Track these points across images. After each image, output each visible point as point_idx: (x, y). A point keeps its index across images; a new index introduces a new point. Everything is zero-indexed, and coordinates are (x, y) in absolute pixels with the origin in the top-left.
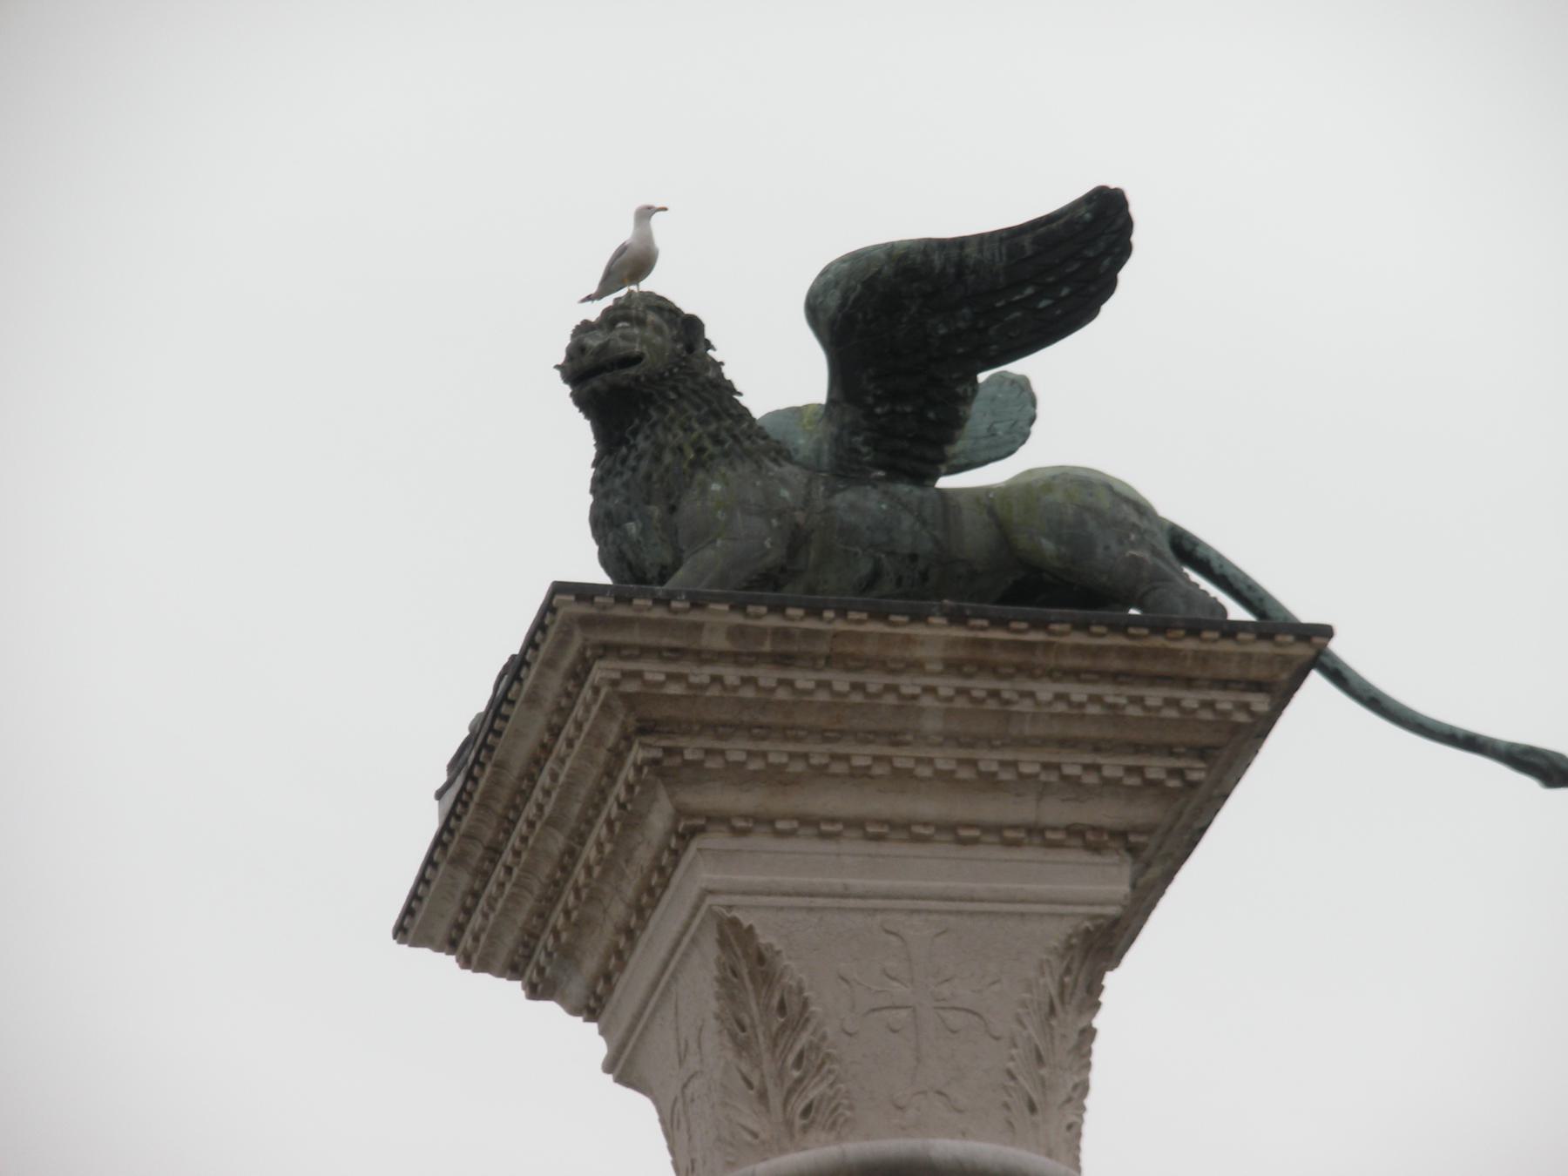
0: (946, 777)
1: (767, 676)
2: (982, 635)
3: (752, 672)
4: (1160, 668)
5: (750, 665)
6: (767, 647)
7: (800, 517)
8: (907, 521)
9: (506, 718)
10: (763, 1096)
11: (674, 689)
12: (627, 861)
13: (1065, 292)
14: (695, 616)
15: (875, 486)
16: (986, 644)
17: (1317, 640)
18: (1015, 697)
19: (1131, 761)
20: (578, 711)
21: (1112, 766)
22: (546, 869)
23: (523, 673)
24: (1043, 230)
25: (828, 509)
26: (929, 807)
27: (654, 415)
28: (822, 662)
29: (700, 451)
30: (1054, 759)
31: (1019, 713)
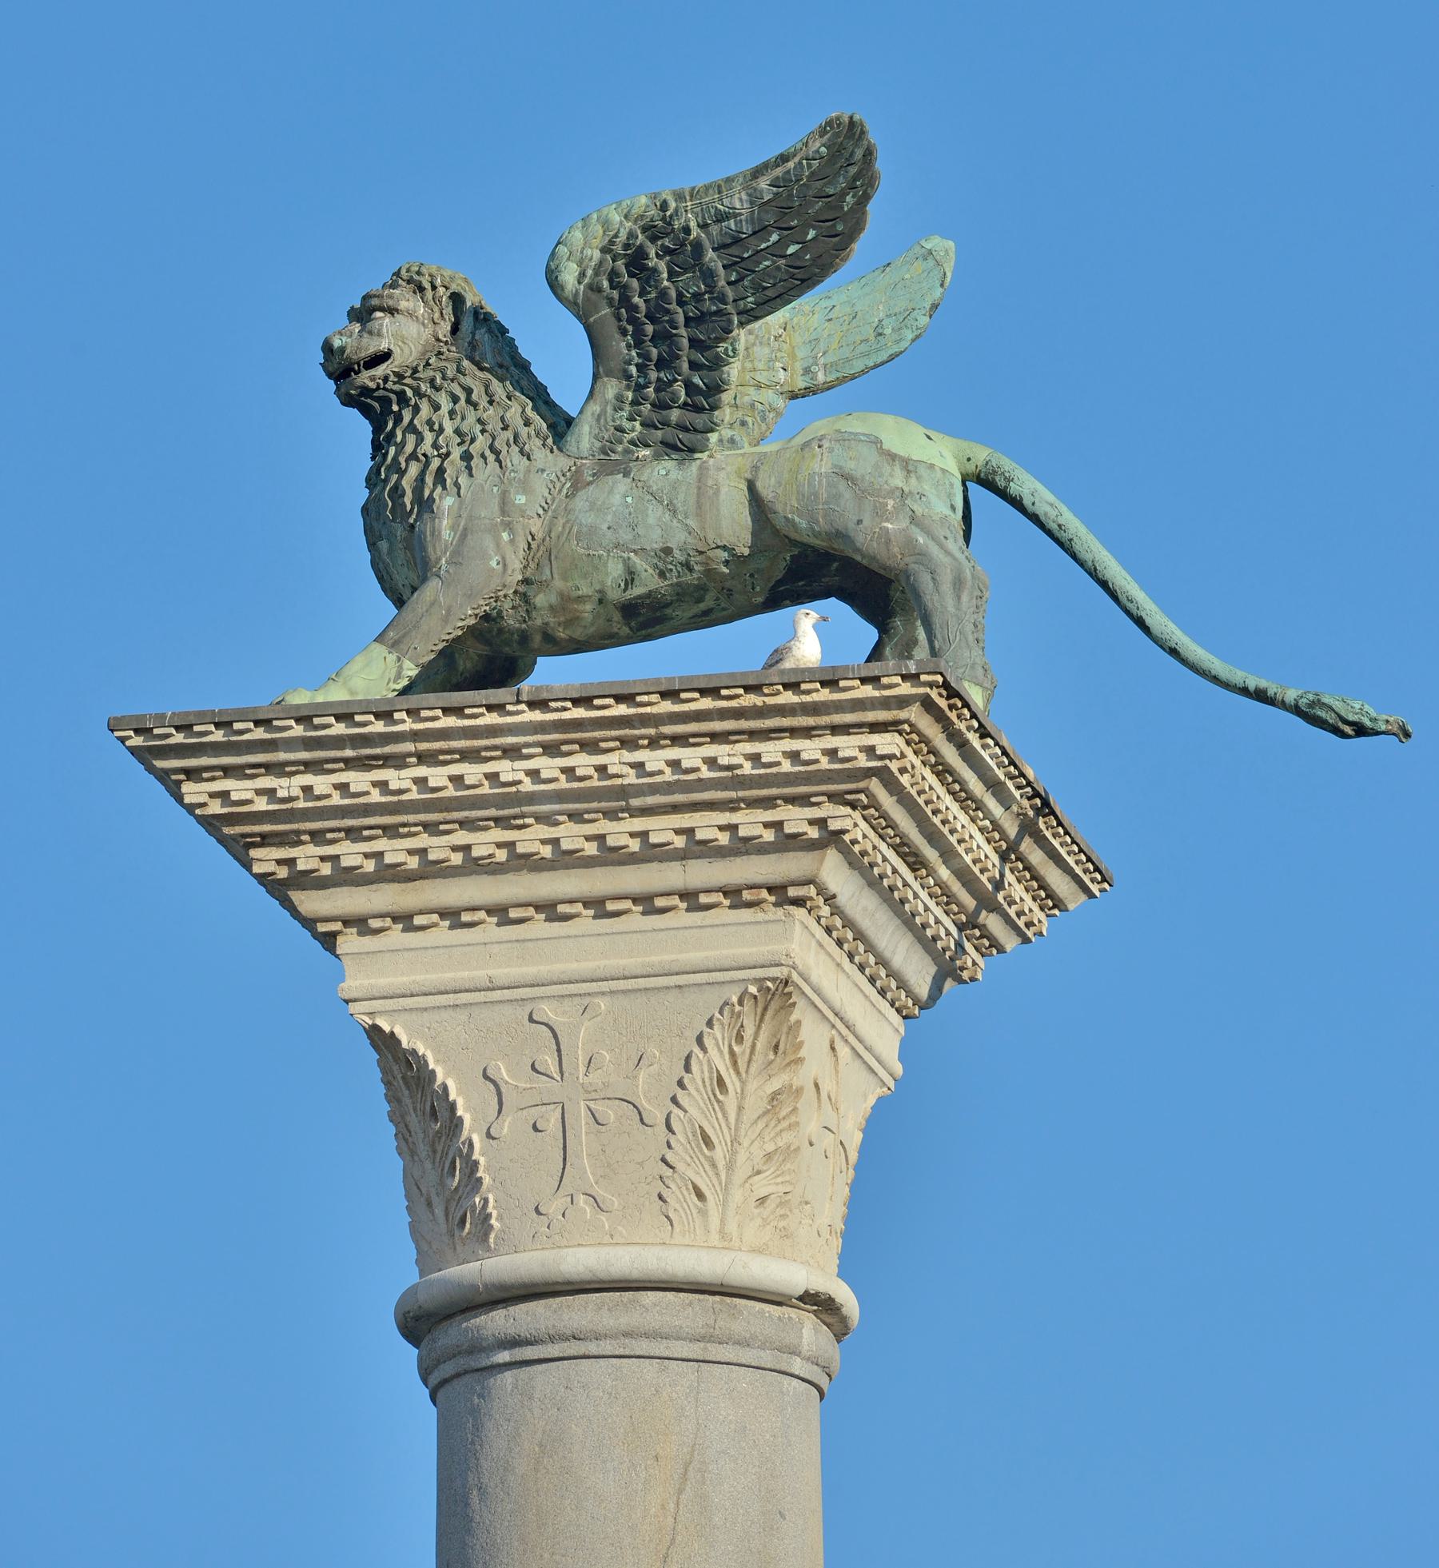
2: (566, 715)
8: (654, 514)
10: (429, 1204)
13: (812, 234)
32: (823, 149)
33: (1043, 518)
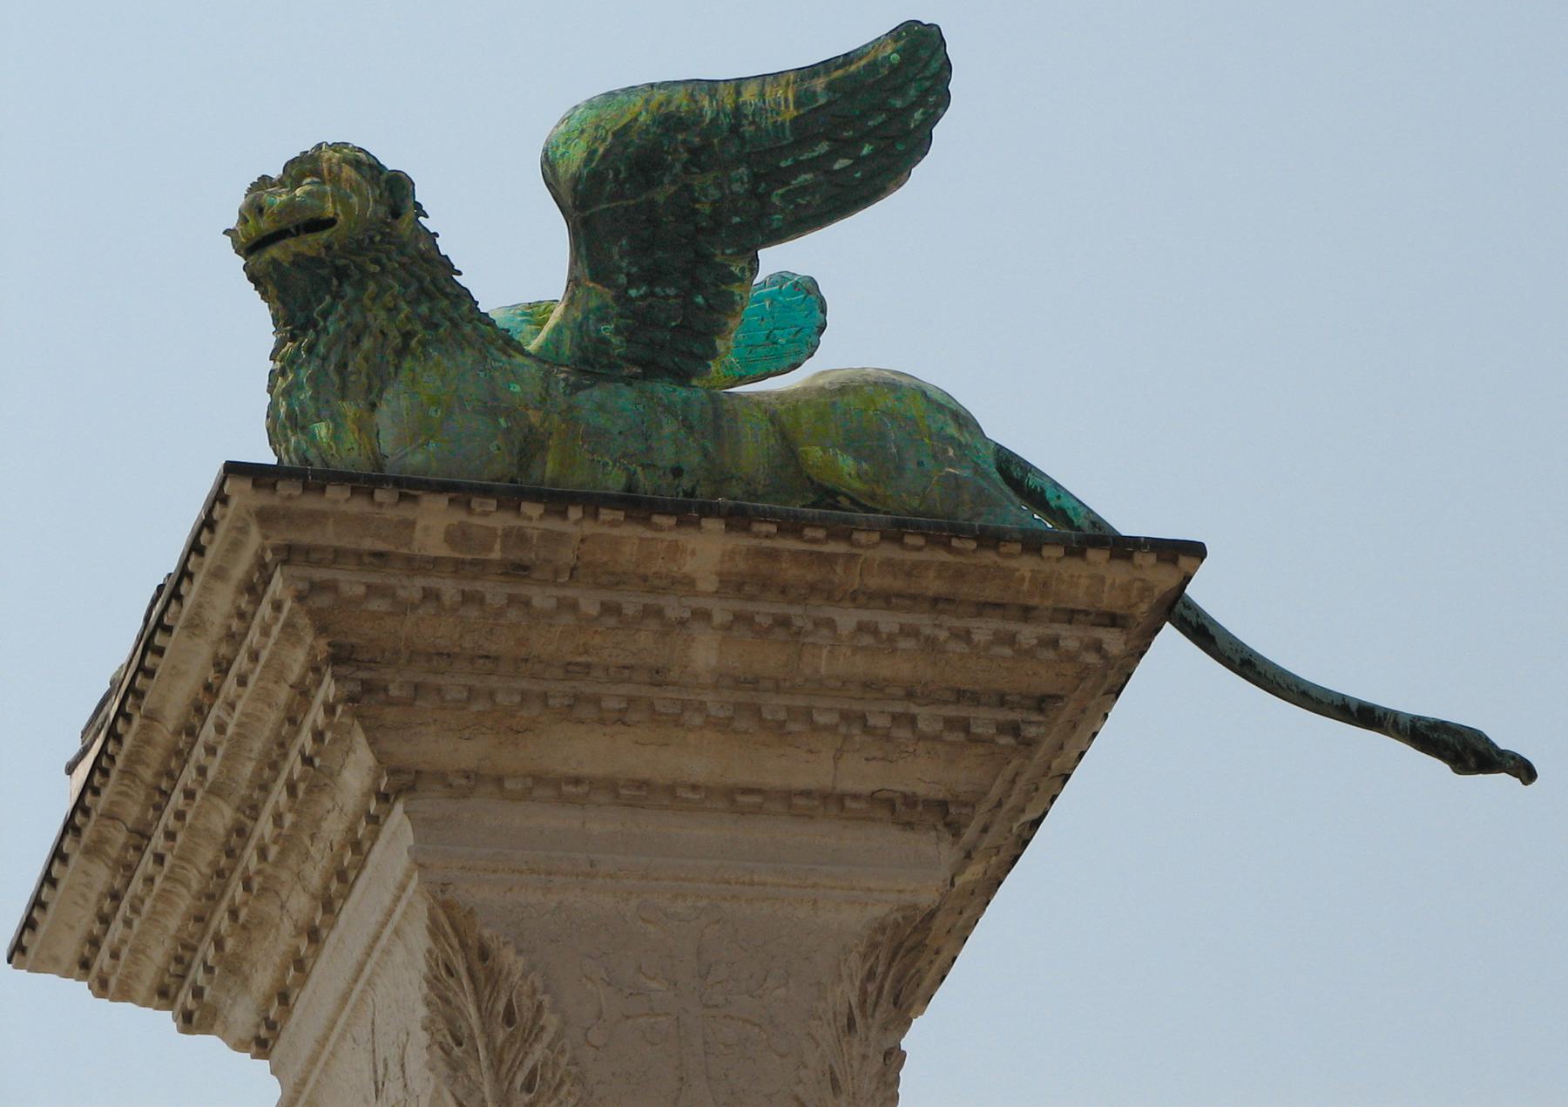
0: (724, 726)
1: (495, 591)
2: (767, 543)
3: (478, 586)
4: (991, 593)
5: (475, 578)
6: (496, 554)
7: (534, 417)
8: (669, 427)
9: (160, 652)
11: (378, 605)
12: (313, 837)
13: (867, 150)
14: (406, 512)
15: (629, 384)
16: (773, 555)
17: (1184, 562)
18: (810, 626)
19: (951, 711)
20: (254, 636)
21: (928, 718)
22: (207, 854)
23: (183, 589)
24: (839, 73)
25: (571, 408)
26: (696, 760)
27: (349, 291)
28: (565, 578)
29: (407, 336)
30: (857, 706)
31: (814, 645)
32: (895, 57)
33: (1071, 513)
